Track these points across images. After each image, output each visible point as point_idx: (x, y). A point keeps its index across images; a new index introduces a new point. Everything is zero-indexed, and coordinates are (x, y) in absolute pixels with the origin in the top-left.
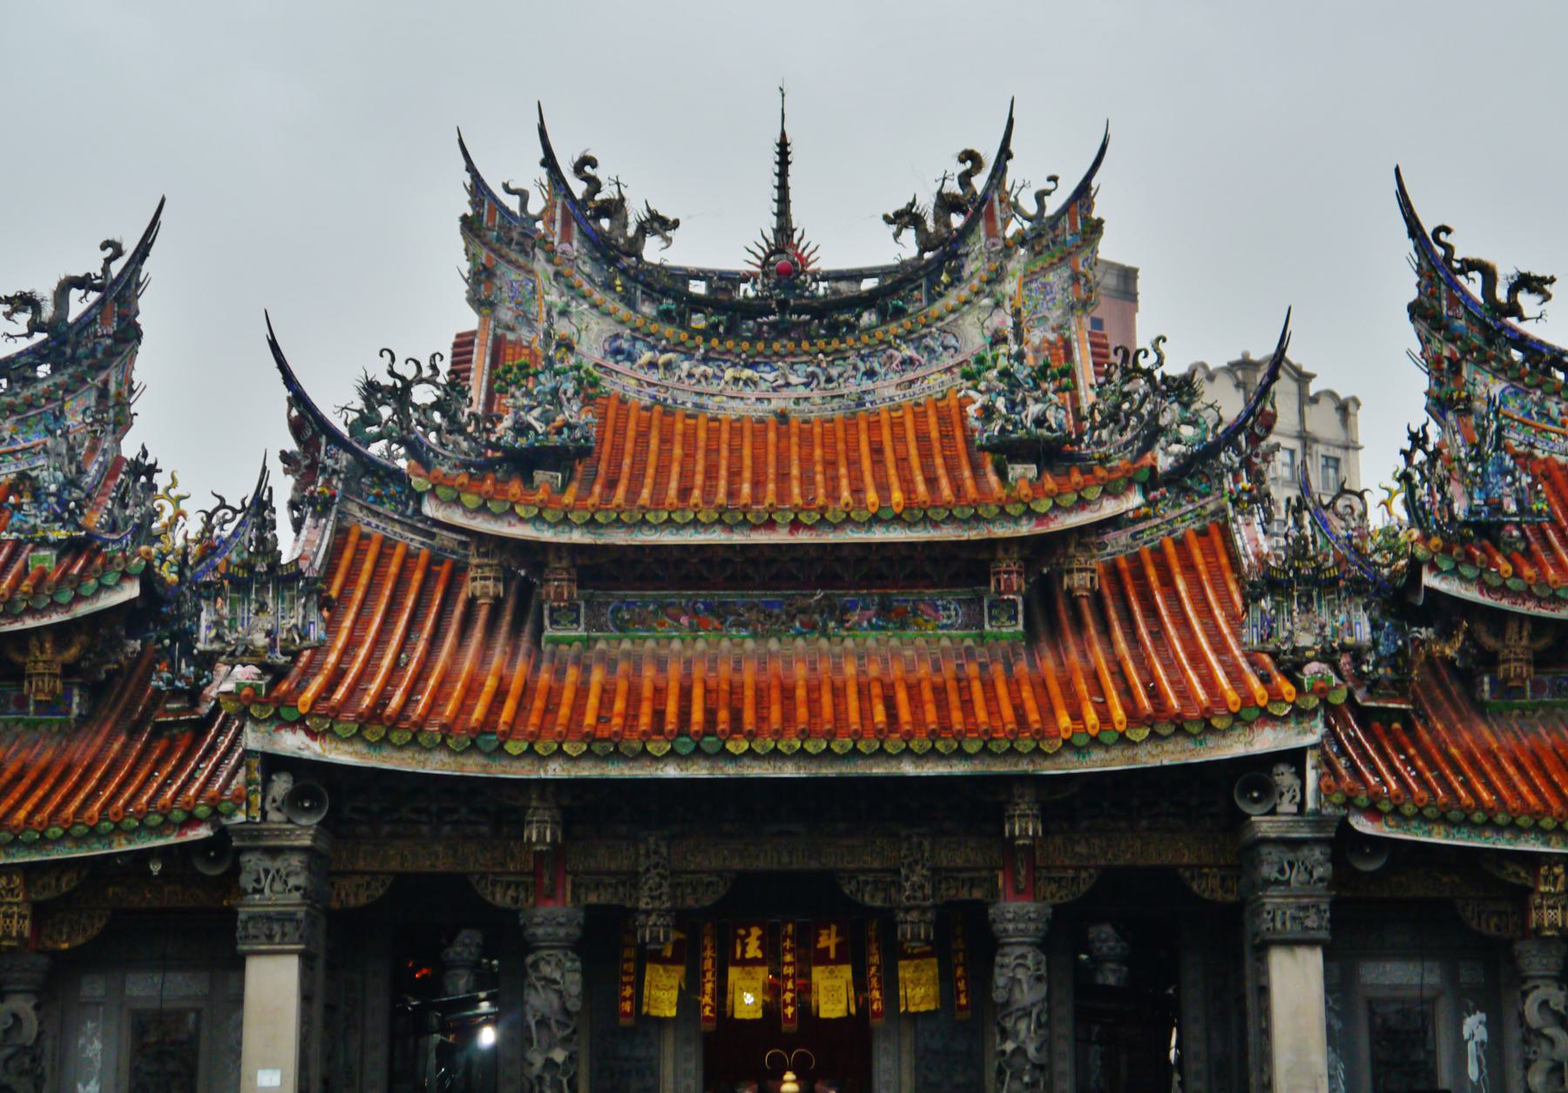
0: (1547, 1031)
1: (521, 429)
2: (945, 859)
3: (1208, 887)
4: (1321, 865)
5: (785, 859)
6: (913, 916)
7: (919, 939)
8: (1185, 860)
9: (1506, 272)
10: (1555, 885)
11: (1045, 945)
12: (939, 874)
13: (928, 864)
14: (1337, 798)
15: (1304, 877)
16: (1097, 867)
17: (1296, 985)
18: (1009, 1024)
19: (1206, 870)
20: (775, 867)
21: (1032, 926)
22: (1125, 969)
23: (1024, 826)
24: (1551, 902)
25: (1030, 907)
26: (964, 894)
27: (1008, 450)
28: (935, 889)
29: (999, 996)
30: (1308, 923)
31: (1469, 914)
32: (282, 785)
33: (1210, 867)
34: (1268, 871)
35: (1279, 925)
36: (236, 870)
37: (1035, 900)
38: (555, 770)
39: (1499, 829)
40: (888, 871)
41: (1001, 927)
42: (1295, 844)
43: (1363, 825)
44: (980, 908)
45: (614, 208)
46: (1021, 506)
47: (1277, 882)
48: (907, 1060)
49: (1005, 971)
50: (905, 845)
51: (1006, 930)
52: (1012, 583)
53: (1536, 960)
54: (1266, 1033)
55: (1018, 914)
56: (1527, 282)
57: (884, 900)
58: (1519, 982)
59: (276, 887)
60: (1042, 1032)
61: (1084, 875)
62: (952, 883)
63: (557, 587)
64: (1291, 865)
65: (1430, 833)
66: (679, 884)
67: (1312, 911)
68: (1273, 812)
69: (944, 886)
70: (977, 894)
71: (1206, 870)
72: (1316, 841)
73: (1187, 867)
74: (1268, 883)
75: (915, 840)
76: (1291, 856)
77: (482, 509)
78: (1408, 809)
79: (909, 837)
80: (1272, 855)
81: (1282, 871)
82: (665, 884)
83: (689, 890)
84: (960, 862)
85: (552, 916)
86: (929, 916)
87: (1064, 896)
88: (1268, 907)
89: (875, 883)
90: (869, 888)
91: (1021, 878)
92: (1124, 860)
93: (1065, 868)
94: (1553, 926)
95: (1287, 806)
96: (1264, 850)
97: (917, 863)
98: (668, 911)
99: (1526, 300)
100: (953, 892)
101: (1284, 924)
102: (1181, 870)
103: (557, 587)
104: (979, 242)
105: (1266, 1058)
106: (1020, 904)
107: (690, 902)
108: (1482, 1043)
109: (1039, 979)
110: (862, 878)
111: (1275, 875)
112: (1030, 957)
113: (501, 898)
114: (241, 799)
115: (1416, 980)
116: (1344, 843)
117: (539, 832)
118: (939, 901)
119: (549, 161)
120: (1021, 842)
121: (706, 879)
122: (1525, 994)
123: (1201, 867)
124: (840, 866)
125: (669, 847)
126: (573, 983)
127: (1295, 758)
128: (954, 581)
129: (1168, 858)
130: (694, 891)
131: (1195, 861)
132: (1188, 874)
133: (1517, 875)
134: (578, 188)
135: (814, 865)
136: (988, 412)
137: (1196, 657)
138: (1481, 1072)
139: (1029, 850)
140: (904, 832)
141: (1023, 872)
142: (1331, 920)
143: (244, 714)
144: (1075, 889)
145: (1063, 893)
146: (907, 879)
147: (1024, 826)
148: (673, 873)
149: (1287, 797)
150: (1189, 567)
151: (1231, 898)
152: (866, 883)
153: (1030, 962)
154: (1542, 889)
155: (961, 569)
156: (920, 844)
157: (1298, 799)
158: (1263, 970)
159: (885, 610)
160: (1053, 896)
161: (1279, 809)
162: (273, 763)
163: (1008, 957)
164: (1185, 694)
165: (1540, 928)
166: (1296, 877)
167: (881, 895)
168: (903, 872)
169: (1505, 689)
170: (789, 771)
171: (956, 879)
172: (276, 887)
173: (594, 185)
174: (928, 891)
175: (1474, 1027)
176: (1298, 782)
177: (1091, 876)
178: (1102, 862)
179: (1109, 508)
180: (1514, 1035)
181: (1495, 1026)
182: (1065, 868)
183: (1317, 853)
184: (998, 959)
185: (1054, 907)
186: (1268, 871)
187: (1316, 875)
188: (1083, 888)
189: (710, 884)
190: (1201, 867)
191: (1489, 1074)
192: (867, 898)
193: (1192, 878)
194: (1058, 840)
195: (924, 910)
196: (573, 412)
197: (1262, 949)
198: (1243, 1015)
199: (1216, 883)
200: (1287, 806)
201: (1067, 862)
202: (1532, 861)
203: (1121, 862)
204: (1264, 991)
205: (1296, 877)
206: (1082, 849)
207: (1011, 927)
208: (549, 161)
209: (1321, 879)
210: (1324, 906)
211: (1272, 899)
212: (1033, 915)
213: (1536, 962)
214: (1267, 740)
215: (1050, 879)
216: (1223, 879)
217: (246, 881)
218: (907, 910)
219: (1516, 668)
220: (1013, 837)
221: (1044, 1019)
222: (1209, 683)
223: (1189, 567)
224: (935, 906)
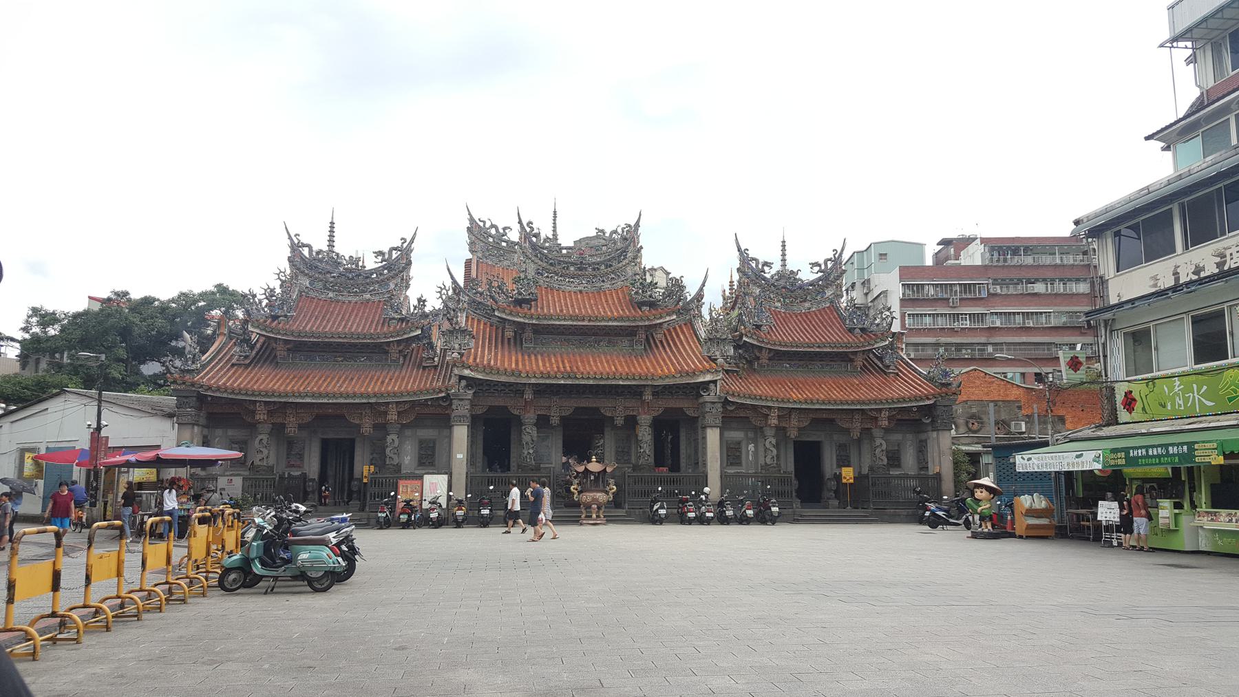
1: (520, 294)
2: (627, 404)
3: (690, 413)
9: (761, 260)
23: (648, 397)
27: (641, 305)
32: (464, 383)
36: (451, 404)
38: (533, 381)
45: (537, 235)
46: (644, 318)
52: (642, 336)
54: (705, 448)
55: (645, 419)
56: (766, 264)
58: (765, 437)
59: (462, 409)
63: (529, 334)
77: (510, 314)
80: (709, 405)
85: (530, 417)
87: (656, 414)
99: (766, 269)
103: (529, 334)
104: (631, 248)
105: (705, 454)
113: (516, 412)
114: (452, 387)
116: (726, 402)
117: (528, 396)
119: (520, 222)
126: (535, 434)
127: (715, 382)
128: (627, 335)
134: (528, 230)
136: (637, 293)
137: (688, 355)
143: (454, 365)
147: (648, 397)
150: (683, 332)
155: (630, 332)
159: (609, 342)
162: (461, 378)
164: (688, 365)
166: (714, 411)
169: (761, 366)
170: (591, 382)
172: (462, 409)
173: (532, 229)
175: (751, 447)
179: (668, 318)
196: (533, 290)
197: (704, 428)
202: (769, 408)
204: (704, 438)
205: (714, 411)
208: (520, 222)
213: (769, 432)
214: (708, 378)
217: (454, 407)
219: (764, 361)
222: (694, 363)
223: (683, 332)
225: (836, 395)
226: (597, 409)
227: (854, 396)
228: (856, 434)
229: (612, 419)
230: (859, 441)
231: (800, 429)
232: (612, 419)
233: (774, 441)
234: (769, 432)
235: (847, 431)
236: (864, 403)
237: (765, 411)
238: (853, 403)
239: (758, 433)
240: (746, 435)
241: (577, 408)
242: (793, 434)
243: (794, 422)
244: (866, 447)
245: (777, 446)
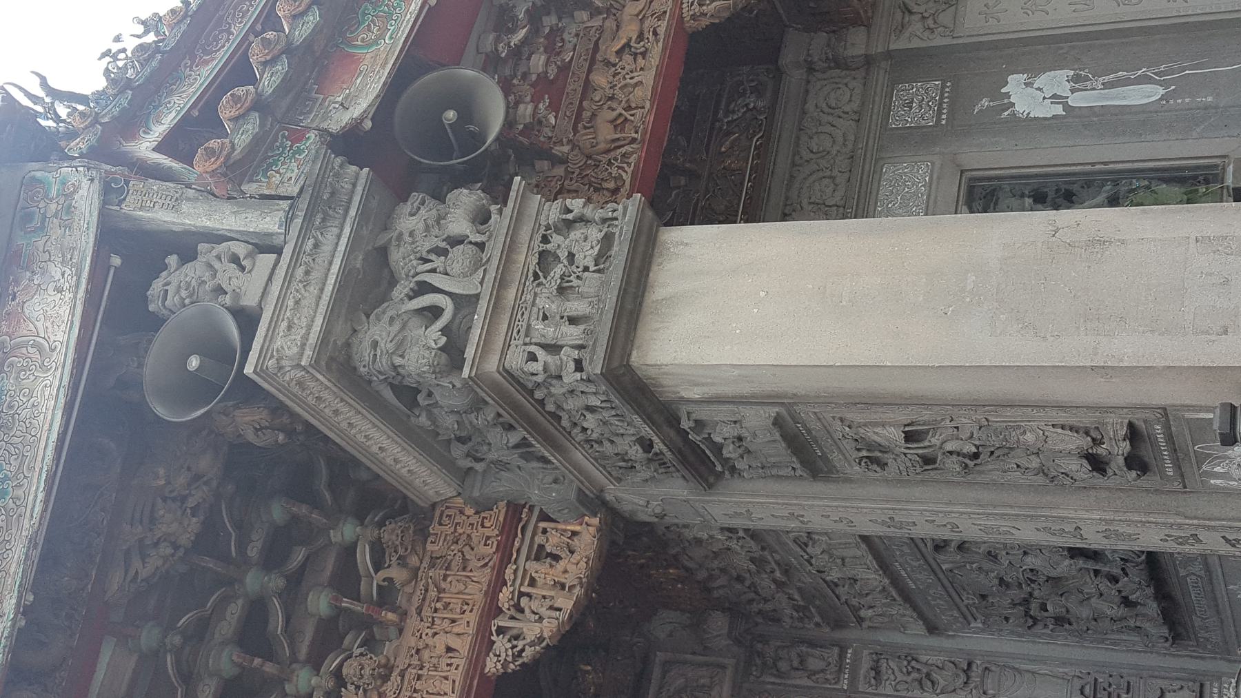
8: (463, 646)
30: (587, 255)
33: (499, 582)
71: (504, 595)
72: (378, 219)
73: (484, 644)
76: (400, 291)
88: (515, 360)
101: (573, 321)
102: (492, 666)
111: (433, 335)
131: (473, 618)
161: (250, 301)
166: (455, 277)
187: (459, 224)
209: (481, 218)
210: (553, 212)
216: (540, 554)
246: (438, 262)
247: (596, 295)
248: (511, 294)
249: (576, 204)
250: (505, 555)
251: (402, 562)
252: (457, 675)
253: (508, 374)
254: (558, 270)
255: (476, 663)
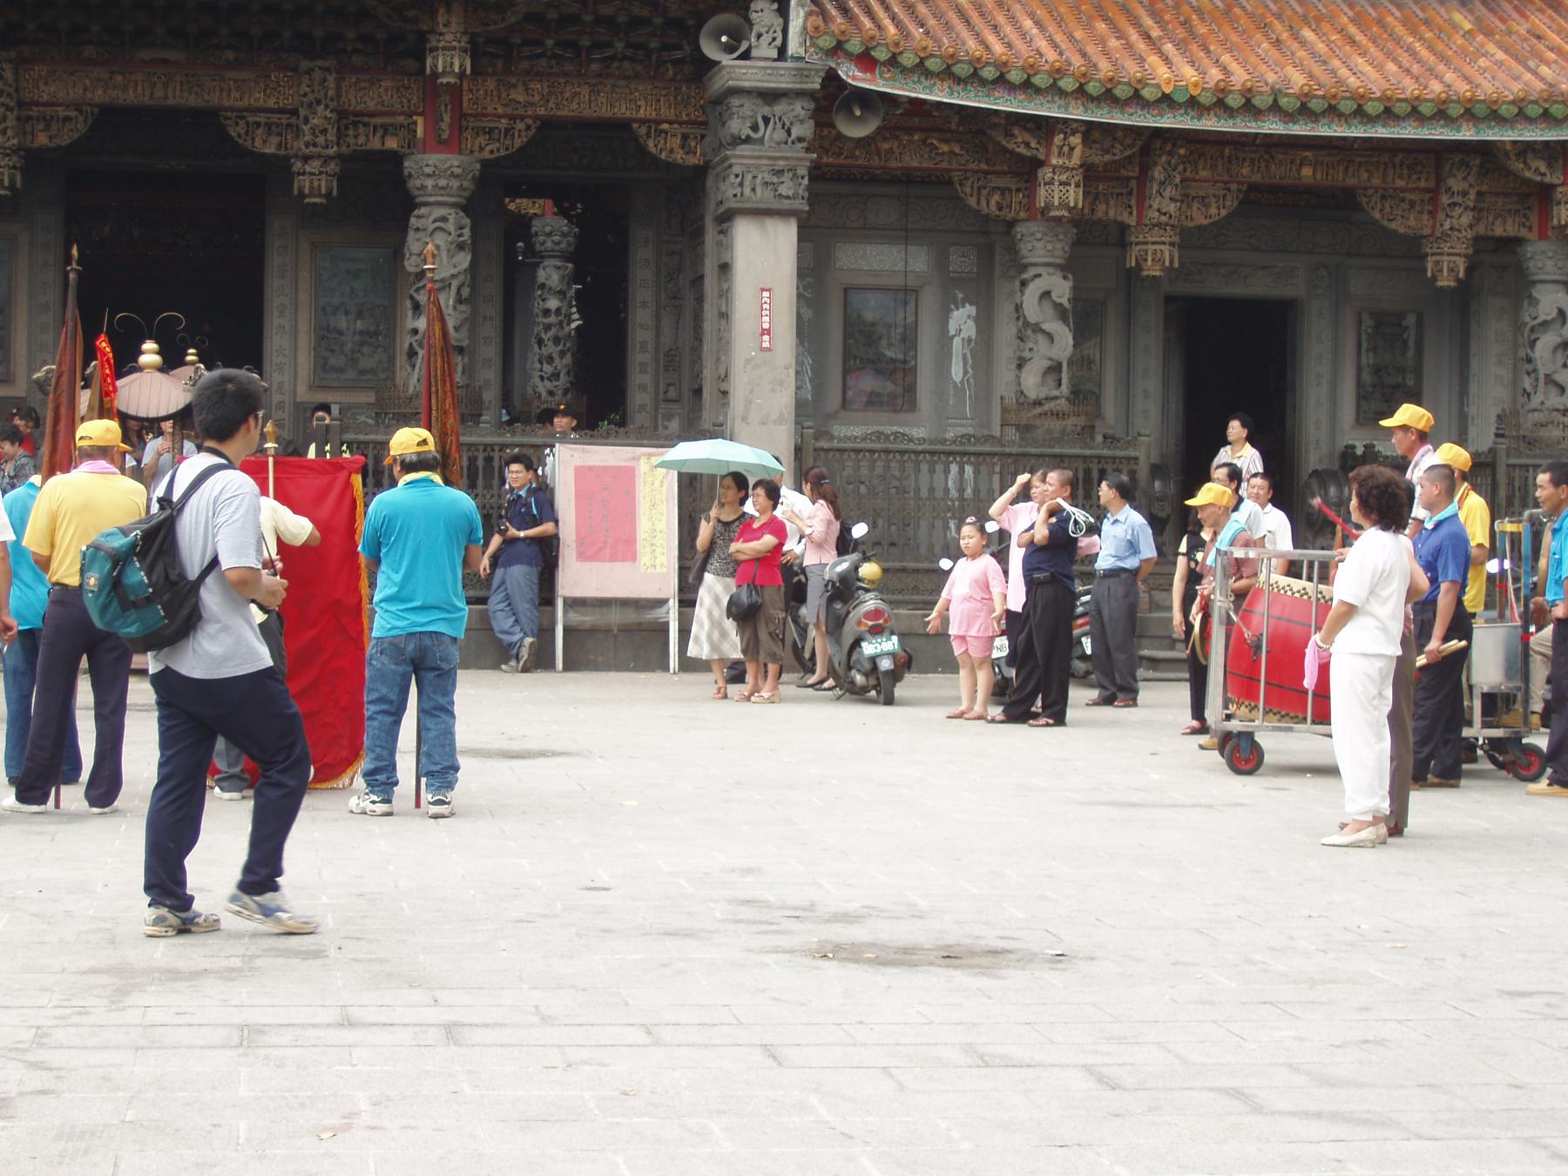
0: (1045, 326)
3: (669, 148)
4: (802, 122)
5: (159, 93)
6: (314, 166)
7: (320, 195)
8: (642, 114)
10: (1070, 156)
11: (466, 208)
12: (346, 119)
13: (333, 105)
14: (827, 42)
15: (780, 135)
16: (536, 118)
17: (762, 265)
18: (422, 298)
19: (665, 126)
20: (147, 101)
21: (455, 184)
22: (570, 266)
24: (1063, 178)
25: (453, 161)
26: (375, 144)
28: (341, 135)
29: (410, 265)
30: (783, 190)
31: (968, 190)
33: (670, 123)
34: (738, 126)
35: (747, 191)
37: (460, 153)
39: (1012, 88)
40: (281, 111)
41: (418, 183)
42: (771, 96)
43: (852, 75)
44: (396, 159)
47: (748, 140)
48: (305, 341)
49: (420, 234)
50: (306, 80)
51: (423, 187)
53: (1039, 245)
55: (439, 172)
57: (279, 146)
60: (463, 308)
61: (520, 126)
62: (361, 130)
64: (766, 120)
65: (930, 89)
66: (29, 118)
67: (787, 177)
68: (746, 56)
69: (351, 133)
70: (392, 144)
71: (665, 126)
73: (642, 122)
74: (738, 141)
75: (317, 74)
76: (766, 110)
78: (908, 60)
79: (309, 72)
81: (755, 128)
82: (11, 116)
83: (41, 126)
84: (371, 105)
86: (332, 167)
87: (492, 150)
88: (737, 169)
89: (269, 126)
90: (260, 131)
91: (444, 126)
92: (569, 110)
93: (500, 116)
94: (1063, 205)
95: (765, 50)
96: (735, 101)
97: (319, 102)
98: (15, 151)
100: (361, 140)
101: (753, 190)
102: (635, 126)
105: (724, 345)
106: (442, 157)
107: (42, 139)
108: (969, 340)
109: (461, 247)
110: (251, 119)
111: (746, 131)
112: (451, 219)
115: (900, 266)
116: (832, 98)
118: (344, 149)
120: (445, 80)
121: (62, 112)
122: (1024, 284)
123: (659, 122)
124: (226, 103)
125: (16, 73)
129: (622, 111)
130: (47, 128)
132: (643, 130)
133: (1027, 145)
135: (193, 101)
138: (966, 372)
139: (455, 91)
140: (305, 64)
141: (447, 118)
142: (808, 188)
144: (508, 142)
145: (494, 146)
146: (306, 121)
148: (21, 104)
149: (766, 39)
151: (692, 160)
152: (258, 125)
153: (450, 226)
154: (1054, 161)
156: (325, 80)
157: (779, 42)
158: (725, 245)
160: (481, 149)
161: (754, 53)
163: (423, 219)
165: (1048, 207)
167: (275, 140)
168: (302, 112)
171: (366, 125)
174: (332, 137)
175: (962, 320)
176: (781, 21)
177: (528, 128)
178: (542, 111)
180: (1006, 331)
181: (985, 323)
182: (500, 116)
183: (800, 108)
184: (413, 220)
185: (485, 164)
186: (738, 126)
187: (795, 133)
188: (518, 143)
189: (67, 119)
190: (659, 122)
191: (975, 376)
192: (258, 143)
193: (648, 135)
194: (491, 84)
195: (327, 160)
197: (726, 218)
198: (700, 299)
199: (676, 142)
200: (765, 50)
201: (500, 111)
202: (1043, 127)
203: (565, 112)
204: (725, 268)
205: (772, 134)
206: (518, 95)
207: (429, 183)
209: (800, 140)
210: (803, 171)
211: (741, 157)
212: (457, 171)
213: (1040, 247)
215: (478, 131)
216: (685, 137)
218: (306, 159)
220: (435, 75)
221: (466, 292)
224: (340, 157)
225: (1367, 72)
226: (209, 119)
227: (1448, 82)
228: (1447, 265)
229: (280, 168)
230: (1464, 300)
231: (1189, 239)
232: (280, 168)
233: (1062, 289)
234: (1040, 247)
235: (1412, 251)
236: (1494, 116)
237: (1022, 144)
238: (1441, 114)
239: (988, 258)
240: (941, 264)
241: (109, 117)
242: (1156, 254)
243: (1163, 203)
244: (1491, 334)
245: (1083, 318)
246: (779, 125)
247: (763, 196)
248: (765, 162)
249: (806, 182)
250: (681, 123)
251: (675, 74)
252: (628, 114)
253: (730, 166)
254: (775, 179)
255: (635, 120)
